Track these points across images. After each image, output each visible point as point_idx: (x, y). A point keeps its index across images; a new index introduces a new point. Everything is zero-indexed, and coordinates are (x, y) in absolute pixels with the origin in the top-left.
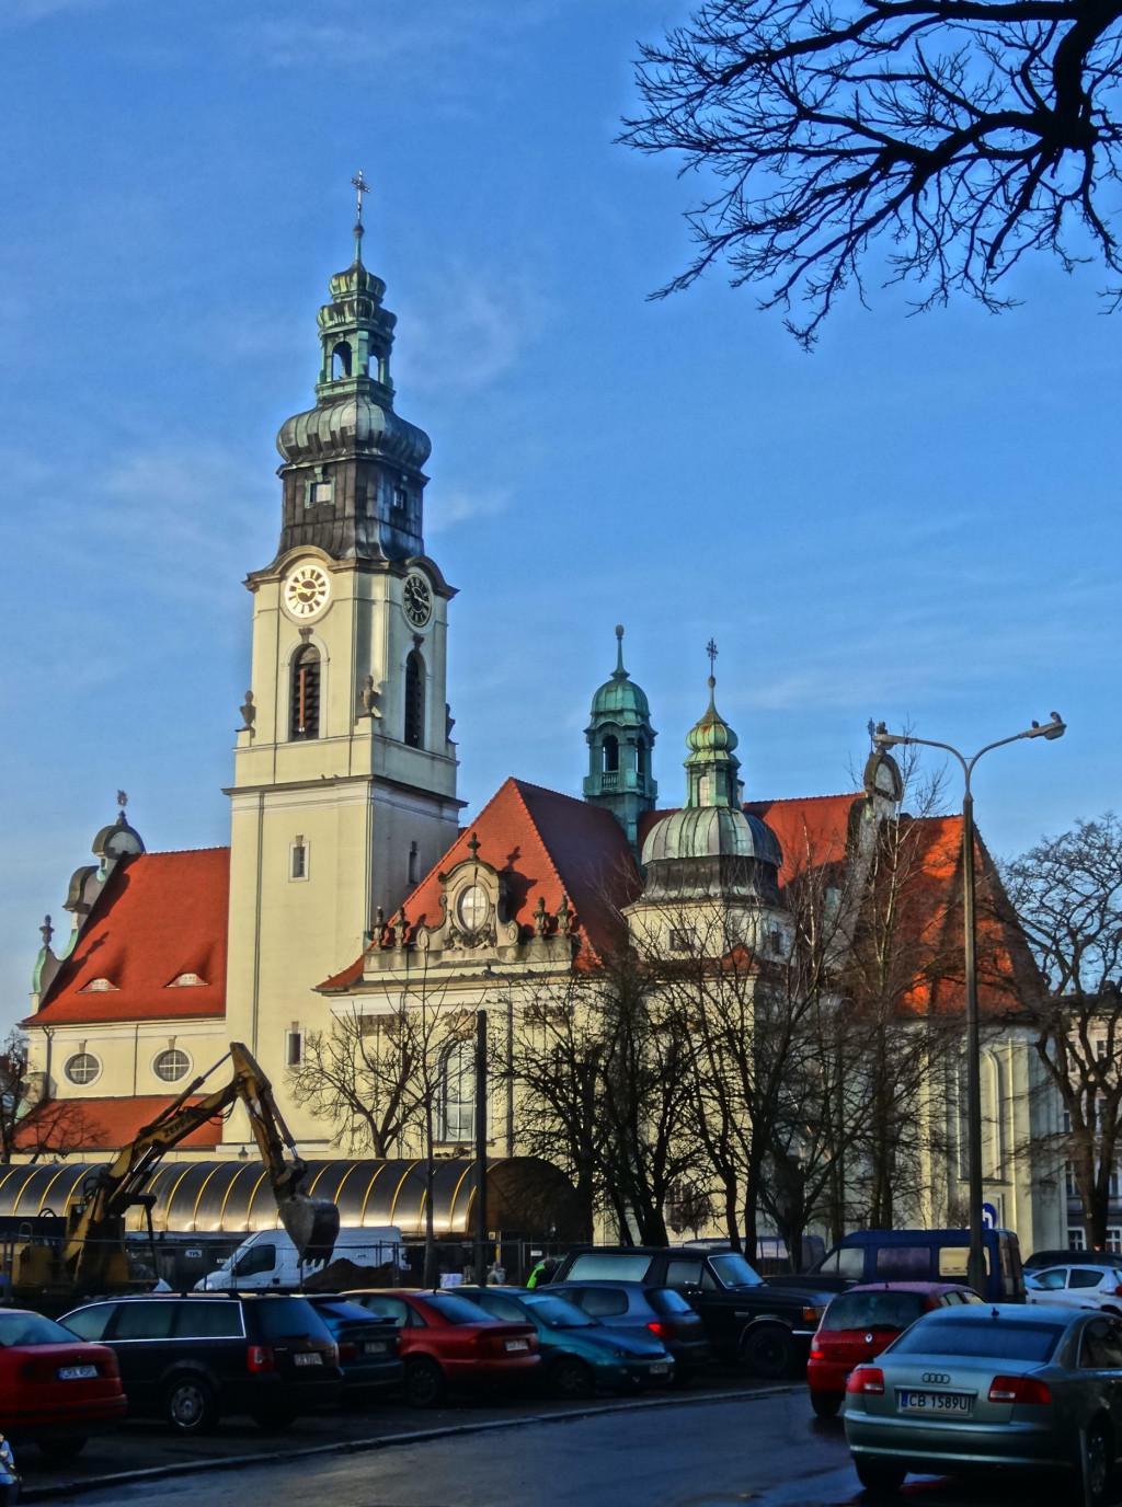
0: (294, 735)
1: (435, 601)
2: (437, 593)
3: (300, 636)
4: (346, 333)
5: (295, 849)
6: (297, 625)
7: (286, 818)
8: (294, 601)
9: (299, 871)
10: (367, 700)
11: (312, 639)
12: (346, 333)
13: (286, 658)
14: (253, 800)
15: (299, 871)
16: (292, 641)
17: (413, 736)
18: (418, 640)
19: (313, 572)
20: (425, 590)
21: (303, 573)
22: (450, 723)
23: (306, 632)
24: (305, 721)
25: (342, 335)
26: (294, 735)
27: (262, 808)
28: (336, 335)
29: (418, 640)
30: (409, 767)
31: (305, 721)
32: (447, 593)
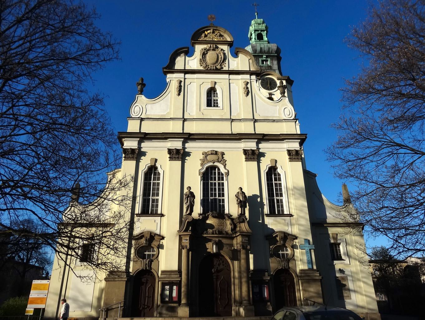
4: (262, 31)
11: (273, 96)
12: (262, 31)
23: (270, 94)
28: (258, 31)
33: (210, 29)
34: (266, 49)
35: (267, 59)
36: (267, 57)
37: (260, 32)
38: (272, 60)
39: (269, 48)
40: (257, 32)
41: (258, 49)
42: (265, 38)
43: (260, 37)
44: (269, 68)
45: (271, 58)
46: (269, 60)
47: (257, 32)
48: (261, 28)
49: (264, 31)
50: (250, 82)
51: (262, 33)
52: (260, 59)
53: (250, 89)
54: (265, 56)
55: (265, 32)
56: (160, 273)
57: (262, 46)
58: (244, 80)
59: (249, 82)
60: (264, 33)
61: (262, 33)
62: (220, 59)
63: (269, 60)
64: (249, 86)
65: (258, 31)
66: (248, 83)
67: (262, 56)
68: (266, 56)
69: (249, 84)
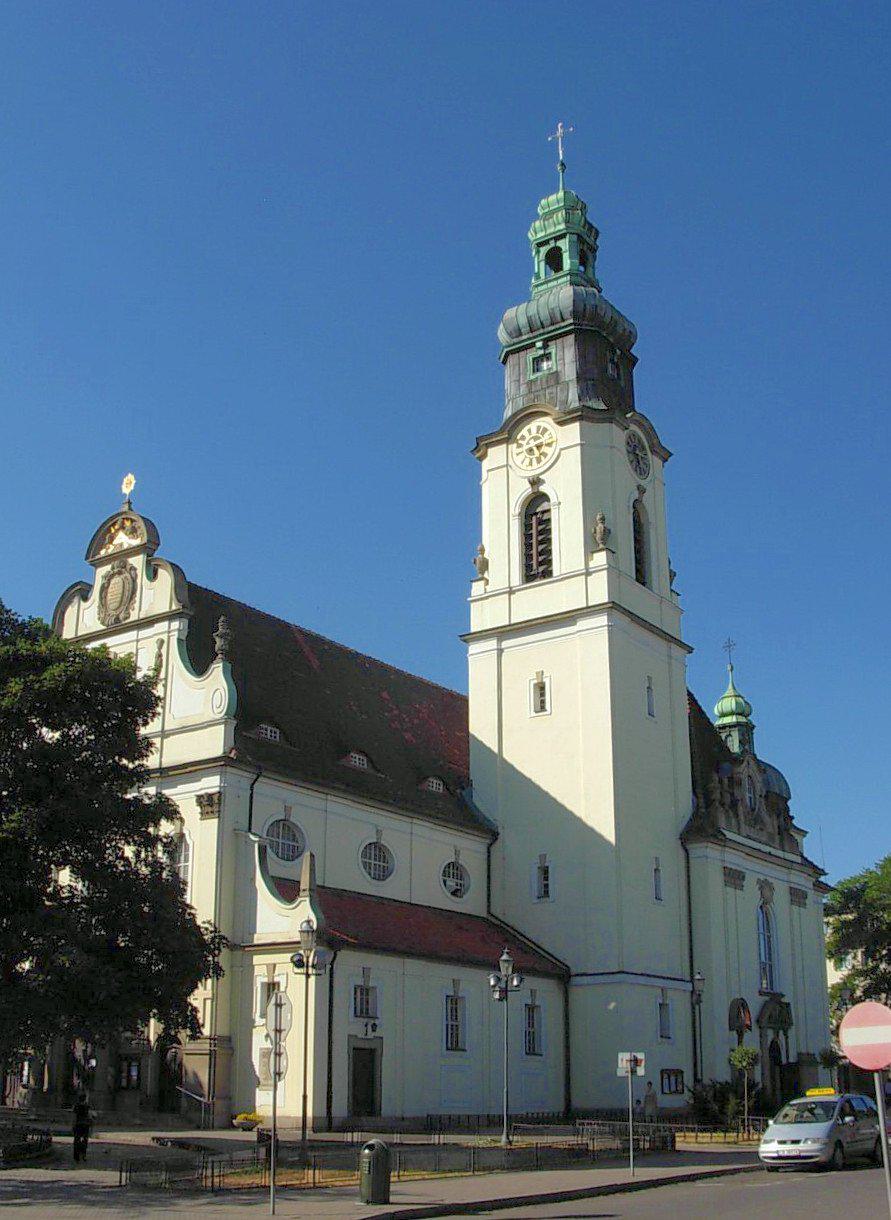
0: (529, 576)
1: (654, 461)
2: (653, 452)
3: (529, 486)
5: (535, 685)
6: (525, 478)
7: (526, 657)
8: (522, 457)
9: (541, 707)
10: (598, 538)
11: (543, 489)
12: (557, 239)
13: (516, 510)
14: (492, 644)
15: (541, 707)
16: (523, 490)
17: (641, 576)
18: (641, 490)
19: (539, 428)
20: (644, 448)
21: (529, 431)
22: (672, 575)
23: (535, 482)
24: (537, 564)
25: (553, 241)
26: (529, 576)
27: (500, 651)
28: (546, 242)
29: (641, 490)
30: (639, 600)
31: (537, 564)
32: (666, 456)
34: (545, 315)
37: (552, 244)
39: (553, 309)
40: (544, 250)
41: (523, 321)
43: (554, 260)
44: (552, 382)
45: (559, 341)
47: (544, 250)
48: (552, 230)
49: (562, 236)
50: (166, 640)
51: (564, 244)
52: (531, 354)
53: (164, 658)
55: (568, 236)
57: (532, 311)
58: (157, 638)
59: (165, 637)
61: (560, 243)
62: (127, 593)
64: (164, 651)
65: (546, 242)
66: (162, 642)
68: (544, 340)
69: (165, 645)
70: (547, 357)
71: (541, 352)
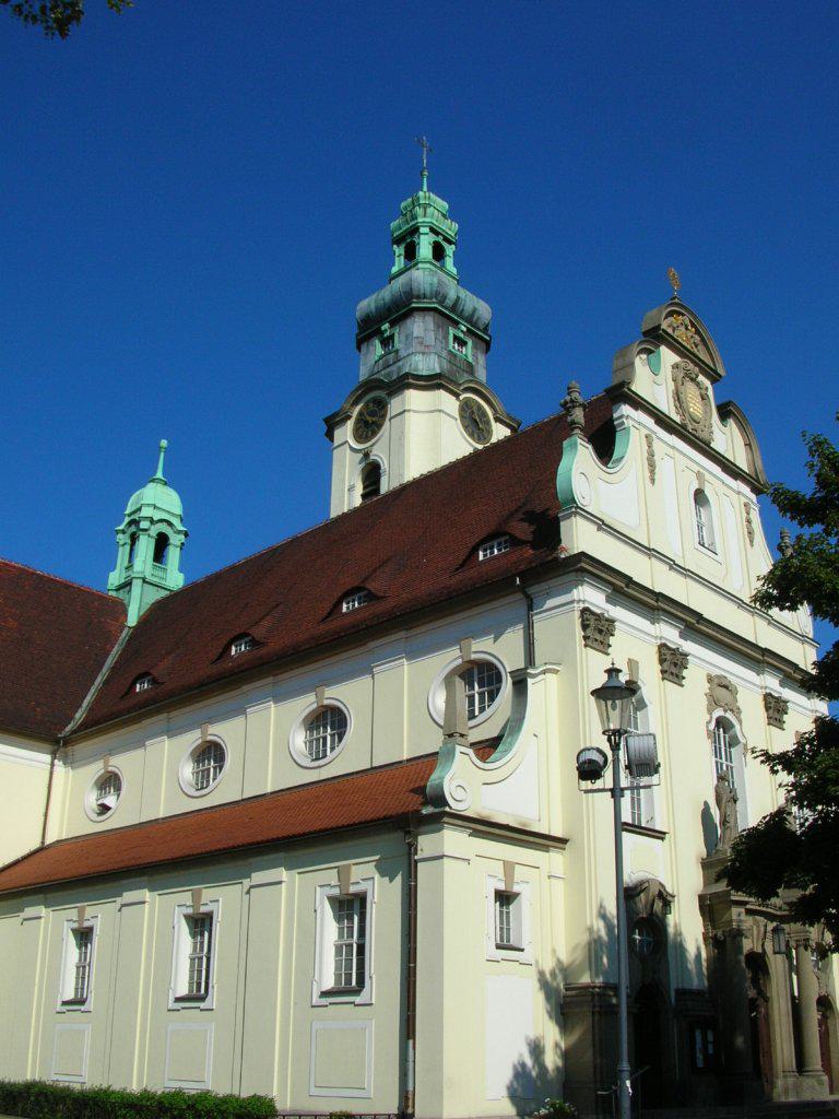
4: (446, 240)
33: (683, 315)
35: (467, 339)
36: (468, 329)
37: (440, 239)
38: (475, 347)
42: (449, 263)
43: (438, 253)
46: (470, 343)
49: (450, 242)
51: (445, 244)
52: (452, 331)
54: (464, 329)
56: (673, 994)
60: (450, 250)
63: (470, 343)
67: (456, 324)
70: (462, 343)
71: (462, 335)
